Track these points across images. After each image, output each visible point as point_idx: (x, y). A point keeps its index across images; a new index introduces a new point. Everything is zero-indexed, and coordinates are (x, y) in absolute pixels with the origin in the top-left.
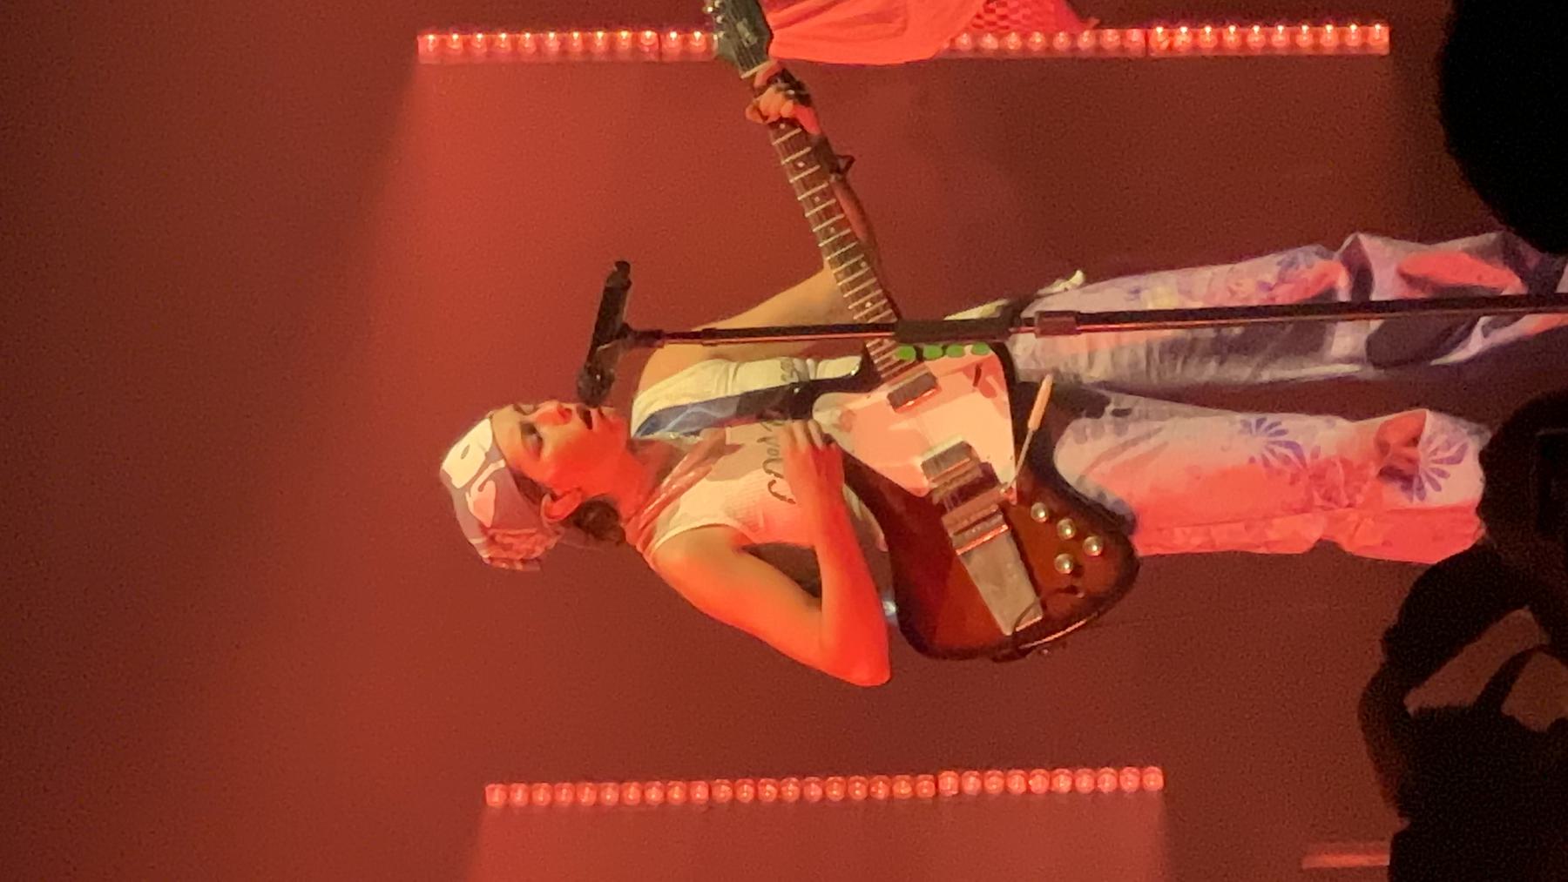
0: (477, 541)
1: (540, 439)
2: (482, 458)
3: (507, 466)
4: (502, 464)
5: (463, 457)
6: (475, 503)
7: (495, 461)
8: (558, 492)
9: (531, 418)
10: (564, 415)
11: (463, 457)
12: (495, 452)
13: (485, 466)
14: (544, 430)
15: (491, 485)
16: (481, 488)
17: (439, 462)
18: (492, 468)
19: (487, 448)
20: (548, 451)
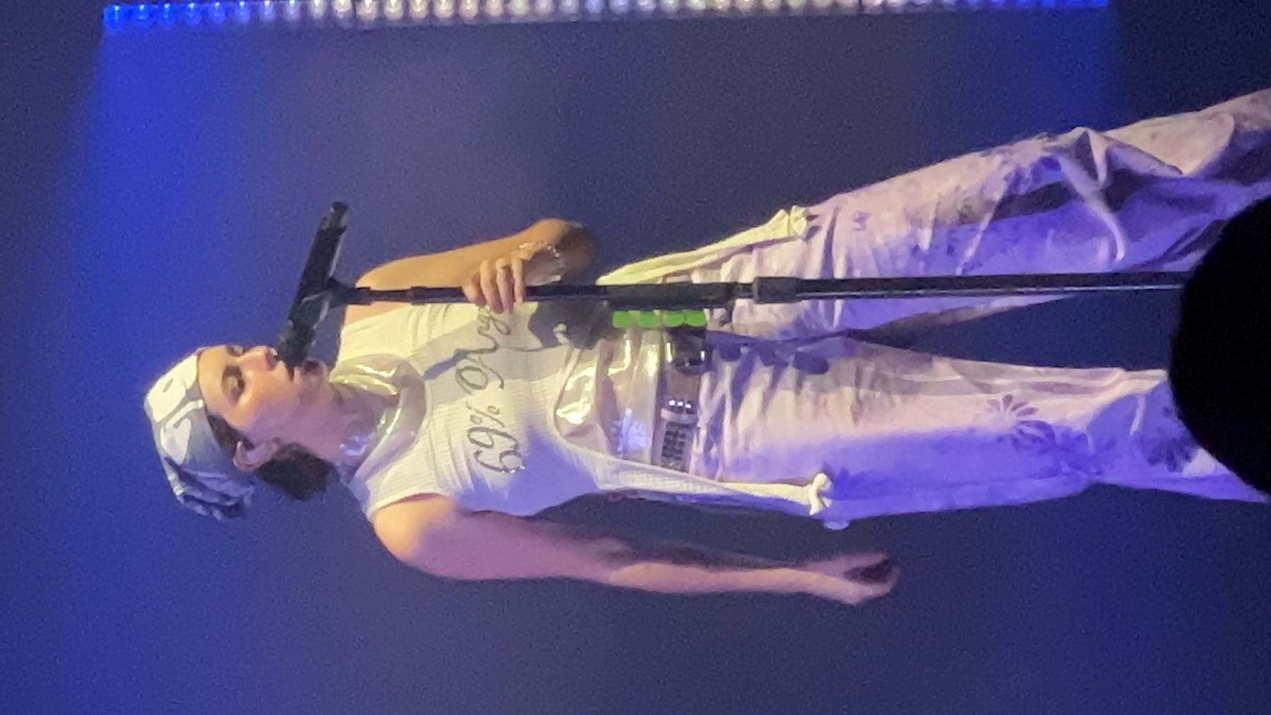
0: (172, 477)
1: (242, 385)
2: (183, 394)
3: (205, 408)
4: (200, 404)
5: (165, 391)
6: (172, 441)
7: (196, 399)
8: (254, 440)
9: (238, 360)
10: (271, 362)
11: (165, 391)
12: (193, 393)
13: (183, 403)
14: (249, 374)
15: (187, 425)
16: (176, 425)
17: (144, 394)
18: (191, 406)
19: (189, 386)
20: (245, 399)
